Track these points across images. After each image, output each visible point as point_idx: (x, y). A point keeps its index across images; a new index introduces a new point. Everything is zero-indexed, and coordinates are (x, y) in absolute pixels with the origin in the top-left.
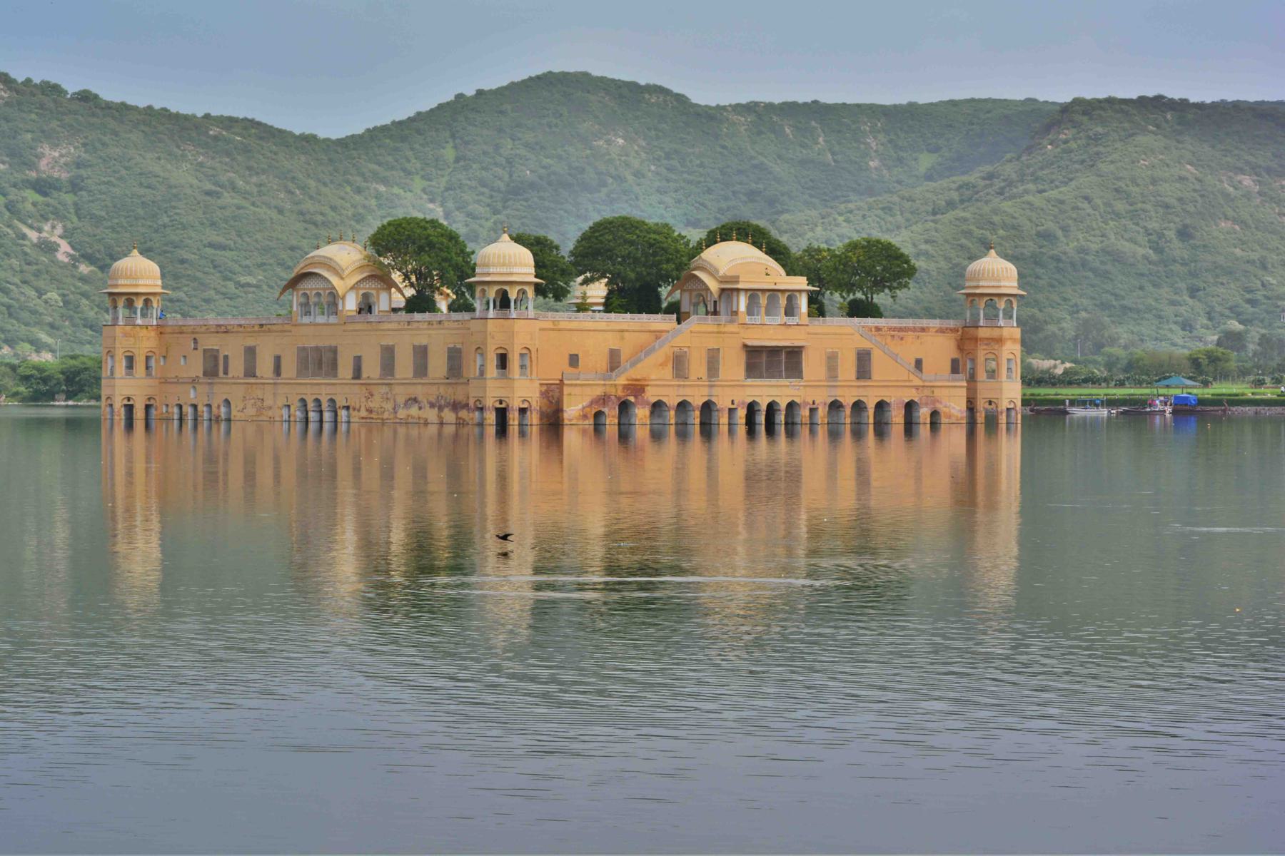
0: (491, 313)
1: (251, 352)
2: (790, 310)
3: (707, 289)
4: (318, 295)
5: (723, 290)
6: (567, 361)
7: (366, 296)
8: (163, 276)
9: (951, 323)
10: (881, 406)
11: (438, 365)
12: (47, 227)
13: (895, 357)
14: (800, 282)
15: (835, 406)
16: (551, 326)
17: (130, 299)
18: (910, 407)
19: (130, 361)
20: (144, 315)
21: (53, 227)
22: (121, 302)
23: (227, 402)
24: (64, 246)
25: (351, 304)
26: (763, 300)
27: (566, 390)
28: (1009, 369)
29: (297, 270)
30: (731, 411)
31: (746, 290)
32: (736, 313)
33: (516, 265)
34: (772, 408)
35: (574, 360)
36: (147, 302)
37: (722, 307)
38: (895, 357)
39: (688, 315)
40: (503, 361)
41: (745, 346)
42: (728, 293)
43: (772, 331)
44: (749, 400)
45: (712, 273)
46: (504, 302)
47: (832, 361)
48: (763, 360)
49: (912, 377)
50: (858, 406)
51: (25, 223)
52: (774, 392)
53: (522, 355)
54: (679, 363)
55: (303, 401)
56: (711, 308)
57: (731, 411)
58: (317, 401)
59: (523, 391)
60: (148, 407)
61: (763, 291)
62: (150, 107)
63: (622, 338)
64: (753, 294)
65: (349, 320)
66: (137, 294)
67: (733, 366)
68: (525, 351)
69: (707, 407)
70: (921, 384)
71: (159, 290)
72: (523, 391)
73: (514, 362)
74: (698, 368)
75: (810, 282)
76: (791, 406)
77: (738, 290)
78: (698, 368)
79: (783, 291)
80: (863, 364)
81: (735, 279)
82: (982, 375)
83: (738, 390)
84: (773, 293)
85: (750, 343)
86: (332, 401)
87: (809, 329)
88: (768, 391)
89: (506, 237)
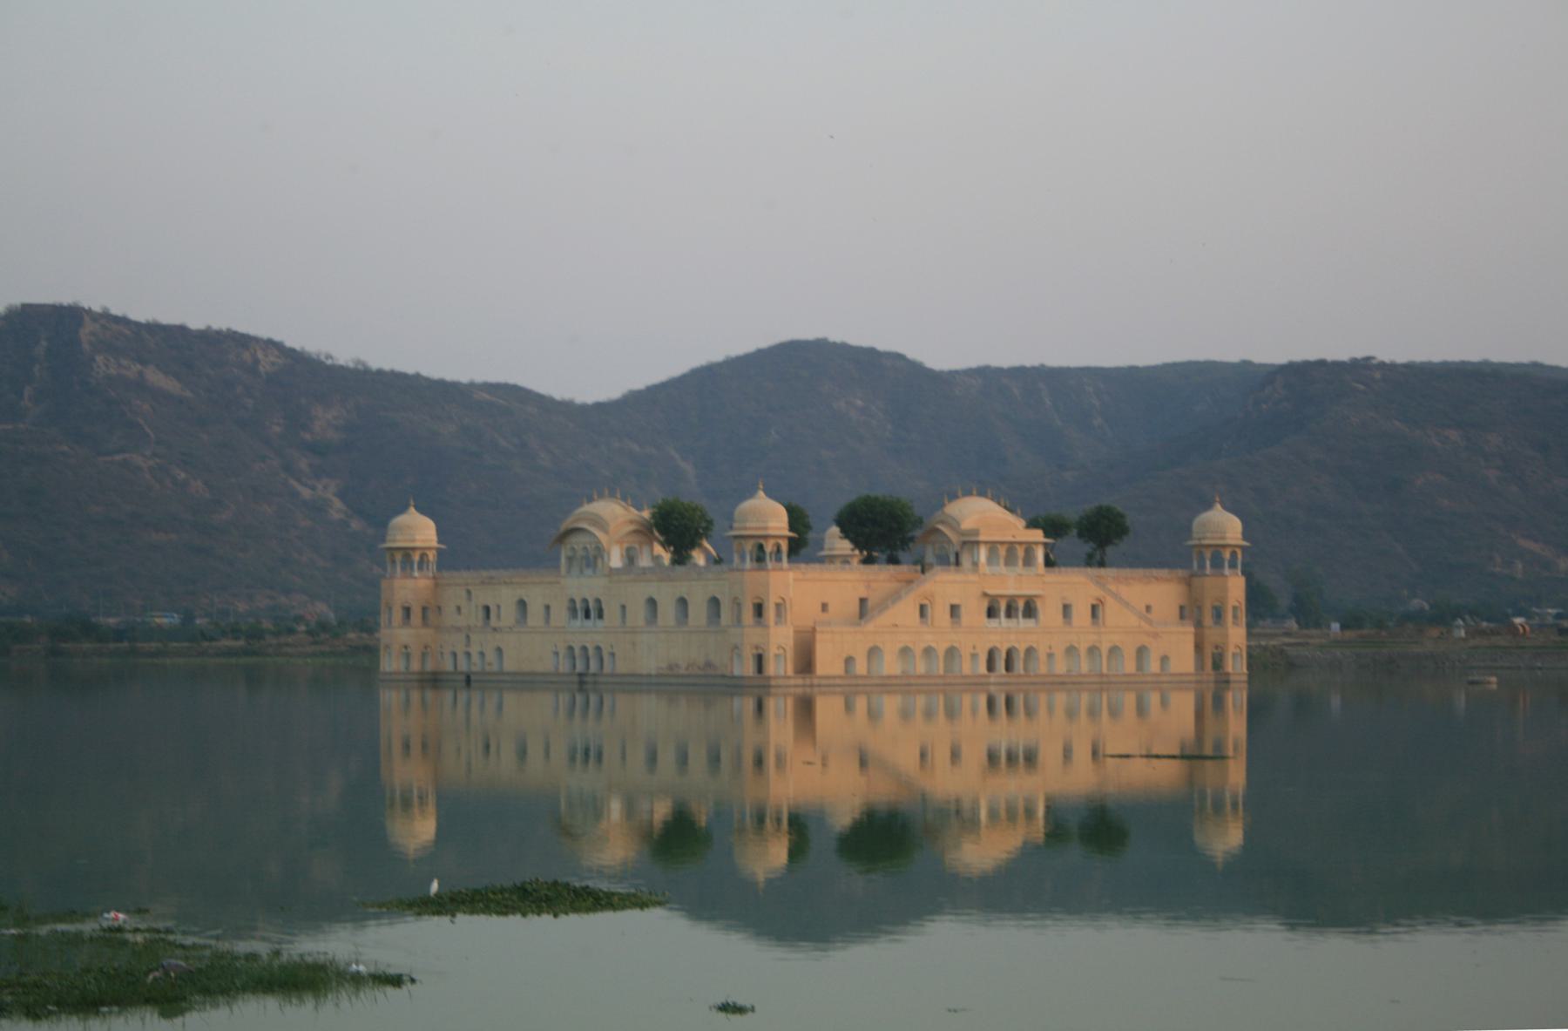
0: (748, 564)
1: (522, 604)
2: (1028, 561)
3: (950, 541)
4: (585, 548)
5: (965, 543)
7: (628, 550)
8: (440, 532)
9: (1181, 573)
10: (1114, 650)
11: (699, 613)
12: (320, 487)
13: (1127, 604)
14: (1037, 535)
17: (407, 552)
18: (1141, 652)
19: (407, 611)
20: (420, 568)
21: (325, 487)
22: (399, 557)
23: (499, 650)
24: (338, 504)
25: (616, 560)
26: (1002, 551)
27: (818, 637)
28: (1235, 617)
29: (564, 527)
30: (974, 656)
32: (975, 564)
35: (824, 607)
36: (423, 556)
37: (966, 560)
38: (1127, 604)
39: (931, 565)
40: (759, 610)
41: (985, 595)
42: (971, 544)
43: (1013, 582)
44: (989, 646)
45: (954, 524)
46: (760, 557)
47: (1067, 609)
51: (299, 480)
53: (778, 605)
55: (571, 649)
56: (952, 559)
57: (974, 656)
58: (584, 649)
59: (780, 640)
60: (424, 655)
61: (1002, 543)
62: (417, 376)
64: (993, 546)
65: (613, 572)
66: (414, 549)
67: (974, 612)
71: (435, 544)
72: (780, 640)
73: (770, 612)
74: (941, 614)
75: (1047, 535)
76: (1030, 651)
77: (978, 543)
78: (941, 614)
79: (1020, 543)
81: (976, 532)
82: (1208, 620)
84: (1011, 546)
85: (991, 592)
86: (598, 649)
89: (761, 493)
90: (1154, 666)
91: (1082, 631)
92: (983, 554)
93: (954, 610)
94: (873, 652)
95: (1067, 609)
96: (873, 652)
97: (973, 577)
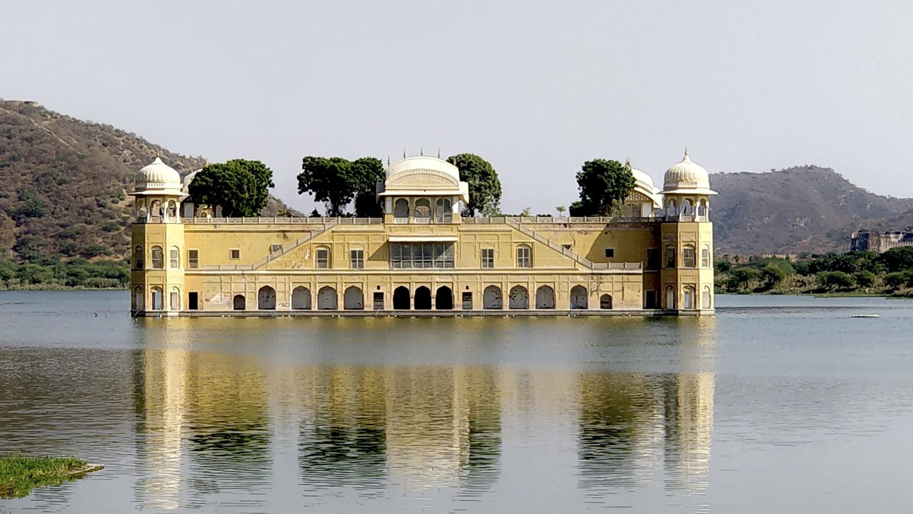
6: (228, 254)
15: (493, 292)
16: (212, 228)
18: (579, 293)
31: (393, 196)
33: (149, 181)
34: (423, 293)
35: (235, 254)
43: (417, 231)
47: (488, 256)
48: (398, 252)
49: (578, 266)
50: (519, 292)
52: (424, 279)
54: (324, 257)
57: (378, 297)
63: (285, 237)
68: (175, 249)
69: (354, 292)
70: (590, 272)
77: (384, 197)
80: (525, 255)
83: (382, 278)
84: (423, 200)
85: (391, 239)
87: (464, 228)
88: (415, 278)
89: (158, 160)
90: (594, 303)
91: (507, 271)
92: (389, 206)
93: (357, 257)
94: (267, 293)
95: (488, 256)
96: (267, 293)
97: (379, 227)
